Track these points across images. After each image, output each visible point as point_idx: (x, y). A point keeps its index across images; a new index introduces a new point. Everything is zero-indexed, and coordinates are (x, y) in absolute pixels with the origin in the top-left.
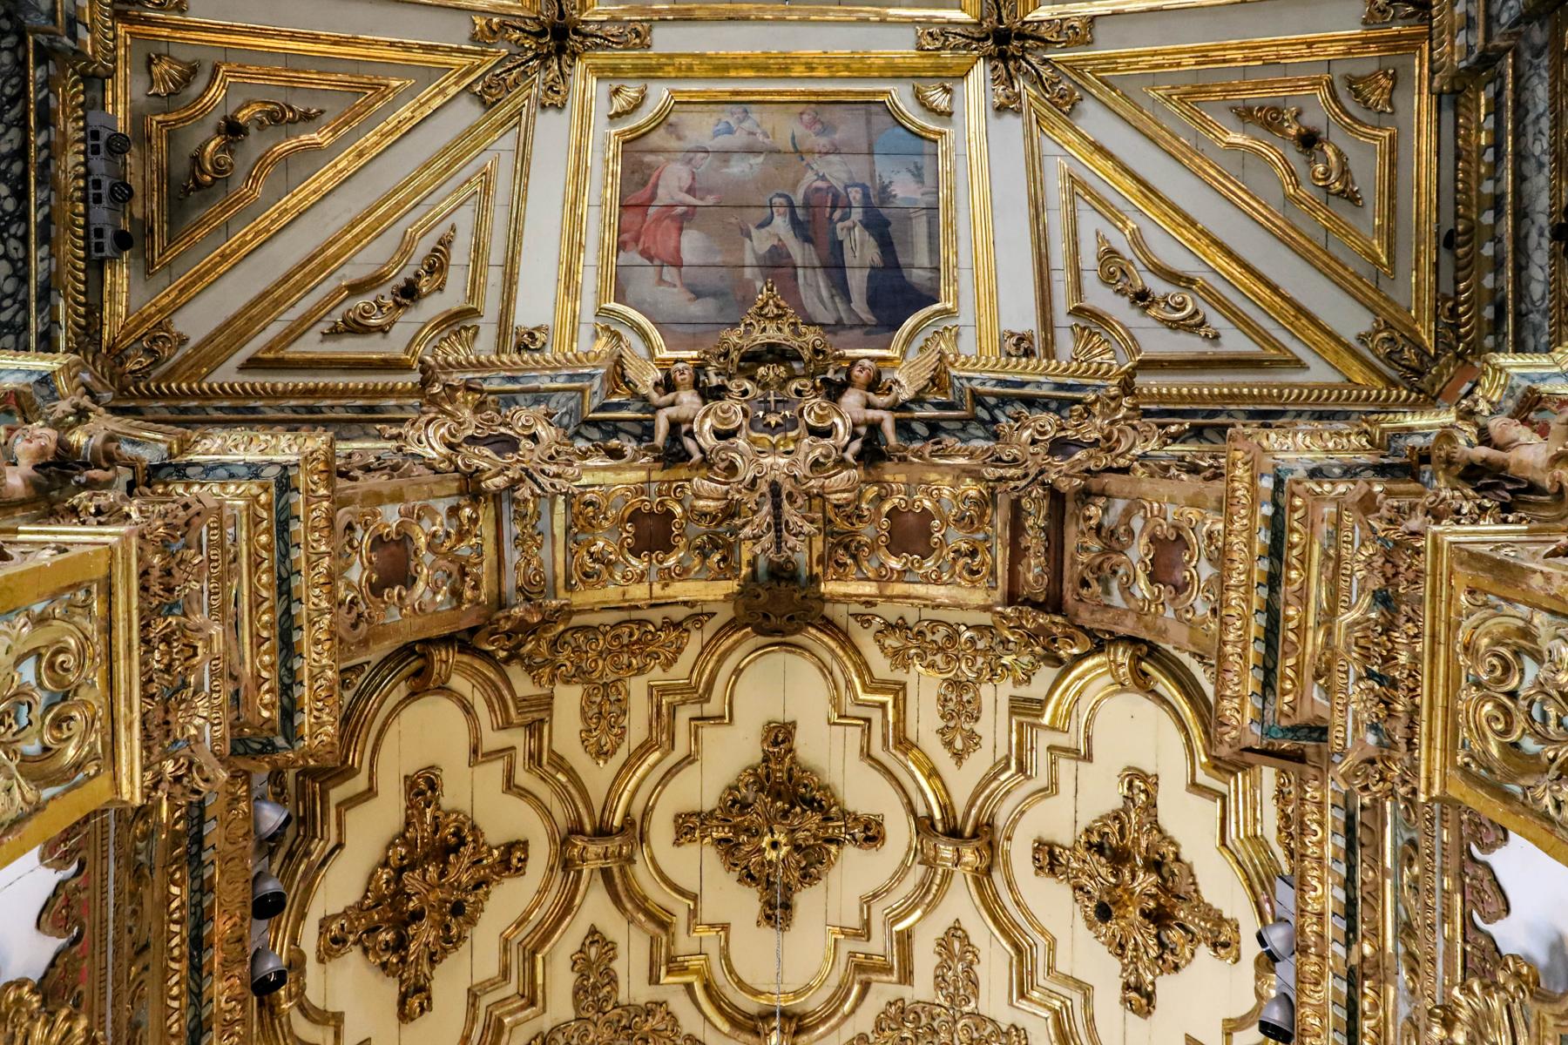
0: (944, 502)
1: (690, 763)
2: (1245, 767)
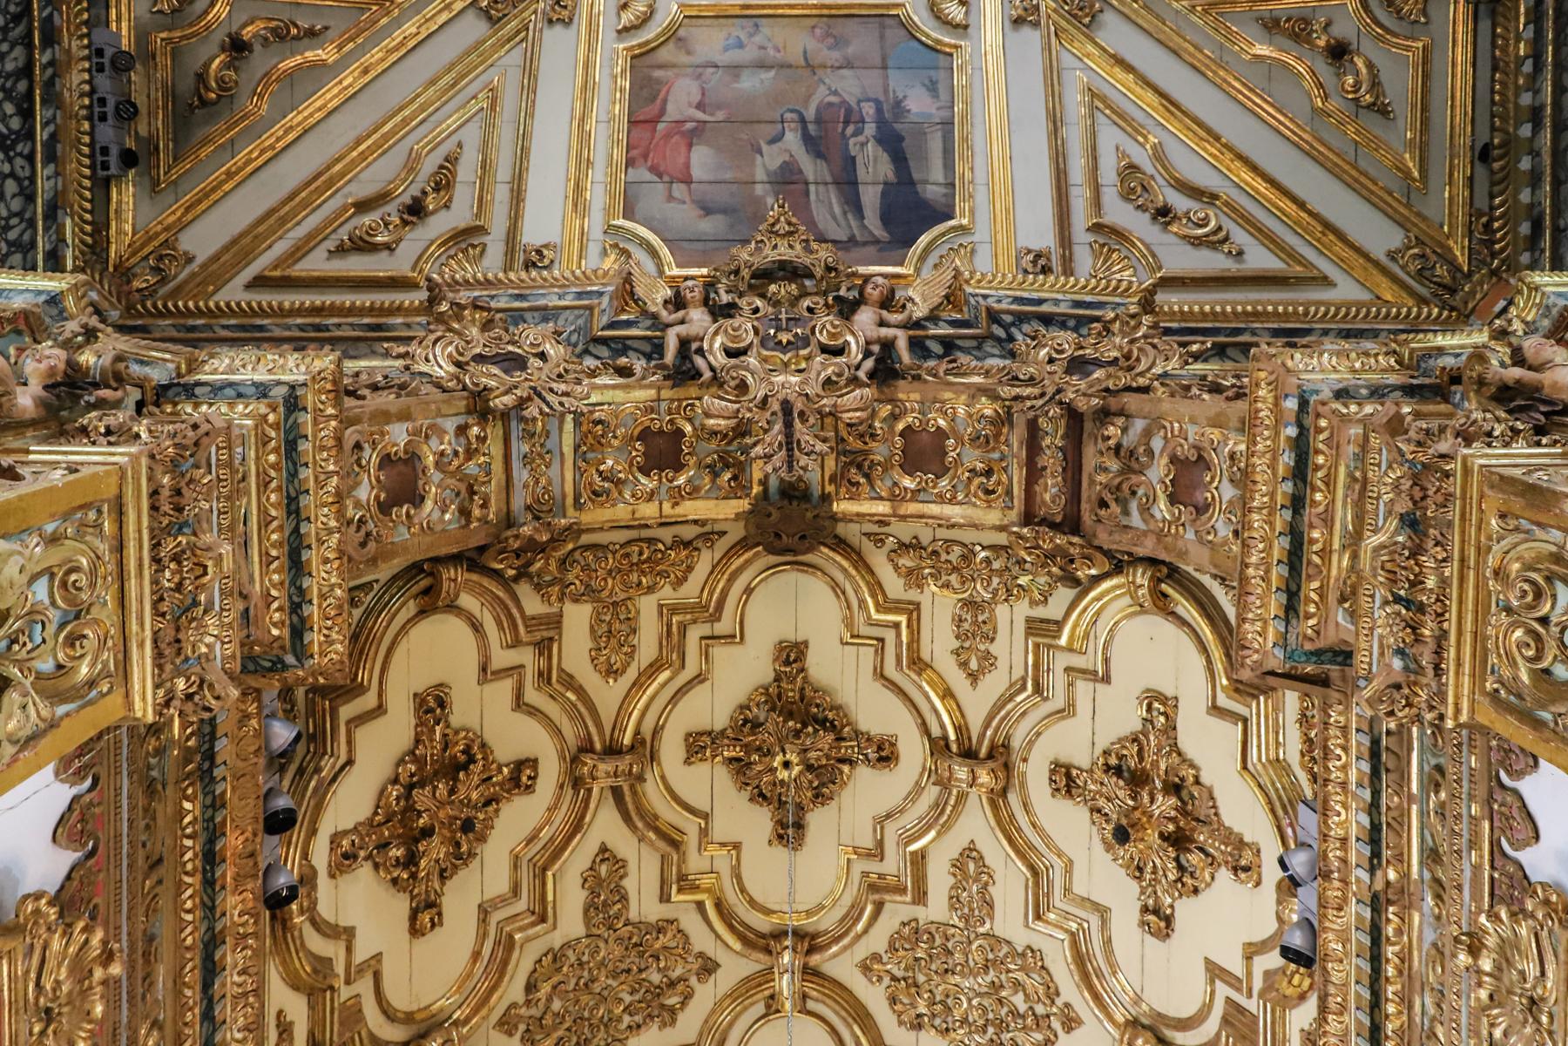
0: (958, 421)
2: (1267, 691)
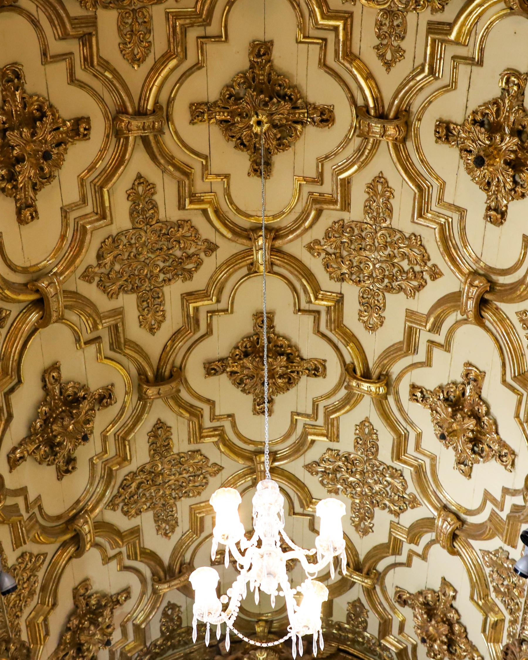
1: (199, 69)
